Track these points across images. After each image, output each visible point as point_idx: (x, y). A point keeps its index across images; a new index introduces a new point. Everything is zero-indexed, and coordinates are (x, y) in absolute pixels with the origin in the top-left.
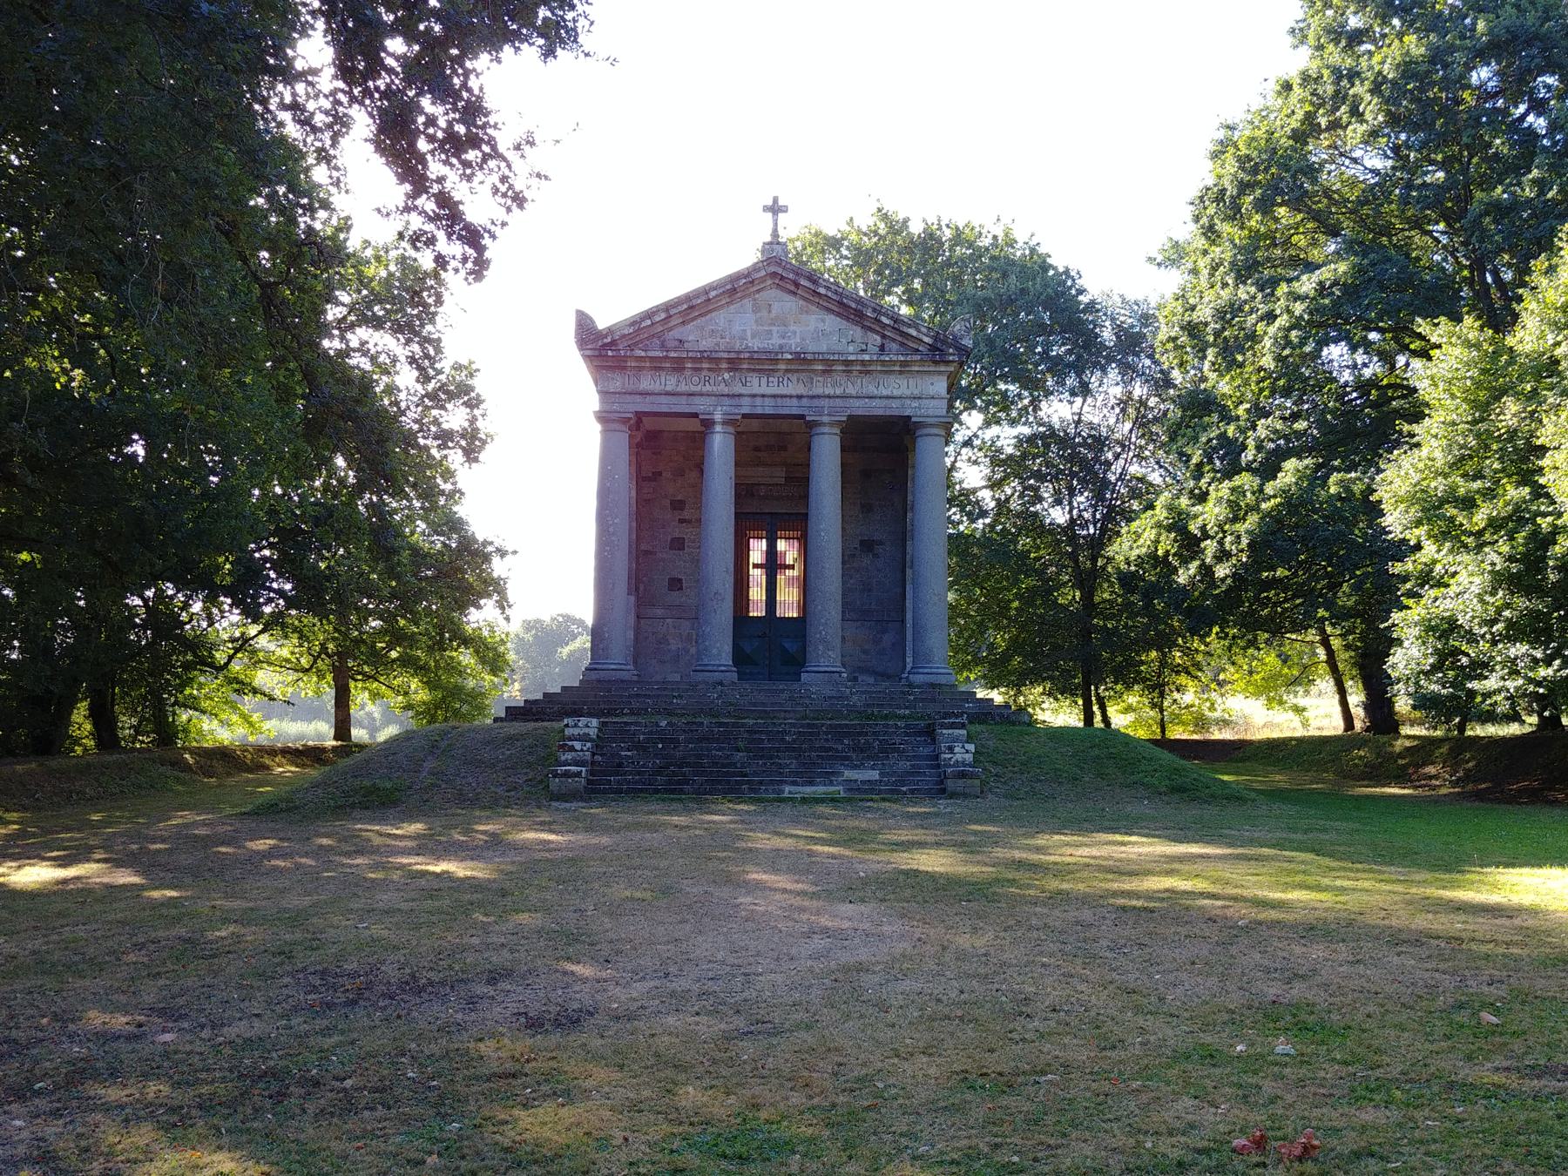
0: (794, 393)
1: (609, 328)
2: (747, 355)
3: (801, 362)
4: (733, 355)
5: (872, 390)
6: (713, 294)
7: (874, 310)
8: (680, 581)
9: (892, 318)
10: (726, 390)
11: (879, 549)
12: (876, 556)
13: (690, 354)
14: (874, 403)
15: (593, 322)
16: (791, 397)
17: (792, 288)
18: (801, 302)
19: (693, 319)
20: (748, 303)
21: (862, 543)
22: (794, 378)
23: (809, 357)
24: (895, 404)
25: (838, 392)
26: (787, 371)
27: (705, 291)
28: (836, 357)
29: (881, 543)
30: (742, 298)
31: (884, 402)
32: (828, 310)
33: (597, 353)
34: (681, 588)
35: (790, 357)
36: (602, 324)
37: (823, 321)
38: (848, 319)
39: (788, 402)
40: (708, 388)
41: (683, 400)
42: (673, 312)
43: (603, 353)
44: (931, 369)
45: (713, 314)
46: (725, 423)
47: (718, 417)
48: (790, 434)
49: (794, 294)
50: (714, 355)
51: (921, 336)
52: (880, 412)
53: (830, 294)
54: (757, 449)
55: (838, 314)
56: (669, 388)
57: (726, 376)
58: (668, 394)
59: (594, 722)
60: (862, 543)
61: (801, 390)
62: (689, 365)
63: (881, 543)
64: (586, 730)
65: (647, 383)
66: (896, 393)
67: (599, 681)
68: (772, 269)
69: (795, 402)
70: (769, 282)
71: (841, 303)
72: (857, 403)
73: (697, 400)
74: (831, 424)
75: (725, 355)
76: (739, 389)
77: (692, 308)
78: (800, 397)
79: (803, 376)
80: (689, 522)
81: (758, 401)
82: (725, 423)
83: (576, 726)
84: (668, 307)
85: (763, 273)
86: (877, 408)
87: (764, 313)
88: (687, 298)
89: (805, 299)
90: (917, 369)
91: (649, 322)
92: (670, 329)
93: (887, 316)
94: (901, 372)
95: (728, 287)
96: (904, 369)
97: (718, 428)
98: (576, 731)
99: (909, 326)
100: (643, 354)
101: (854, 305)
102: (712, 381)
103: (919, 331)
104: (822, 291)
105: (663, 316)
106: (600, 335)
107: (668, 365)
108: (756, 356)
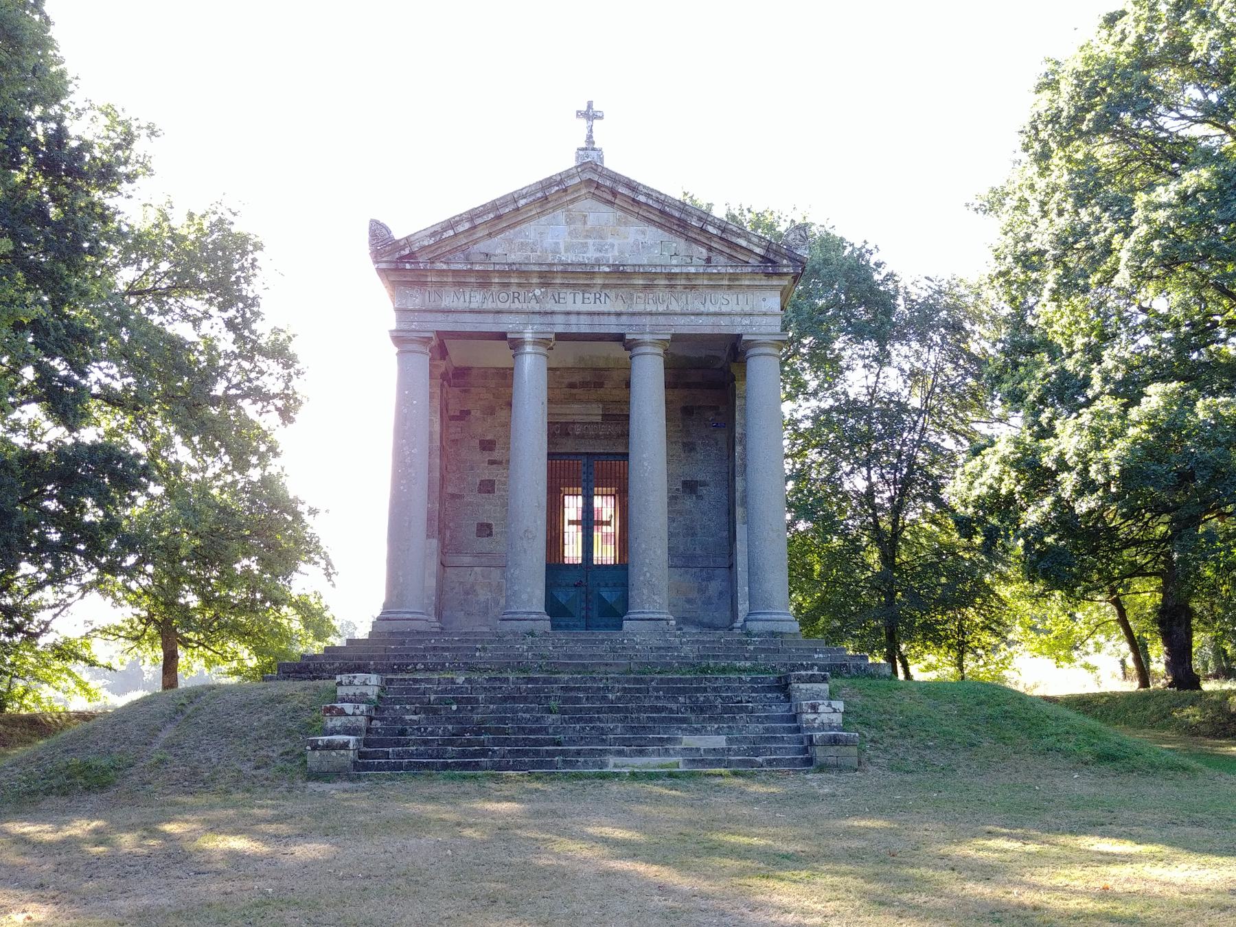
0: (613, 310)
1: (407, 239)
2: (560, 268)
3: (620, 276)
4: (545, 268)
6: (522, 202)
7: (700, 219)
8: (489, 526)
9: (719, 227)
10: (537, 308)
11: (703, 491)
12: (700, 497)
13: (497, 267)
15: (389, 232)
16: (609, 314)
17: (610, 198)
18: (619, 213)
19: (503, 230)
20: (560, 215)
21: (685, 483)
22: (612, 294)
23: (629, 269)
24: (724, 321)
25: (661, 309)
26: (604, 286)
27: (513, 198)
28: (659, 270)
29: (704, 484)
30: (554, 209)
31: (712, 320)
32: (650, 221)
33: (393, 266)
34: (490, 534)
35: (607, 269)
36: (399, 233)
37: (644, 233)
38: (670, 230)
39: (605, 319)
40: (517, 305)
42: (478, 221)
43: (401, 266)
44: (764, 283)
45: (523, 226)
46: (536, 343)
47: (528, 336)
48: (608, 369)
49: (611, 203)
50: (524, 268)
51: (752, 247)
52: (708, 331)
53: (650, 202)
54: (572, 386)
55: (661, 226)
56: (474, 306)
57: (538, 292)
58: (472, 311)
59: (374, 679)
60: (685, 483)
61: (620, 307)
62: (497, 280)
63: (704, 484)
64: (364, 689)
65: (449, 300)
66: (724, 309)
67: (392, 633)
68: (587, 176)
69: (613, 319)
70: (584, 191)
71: (662, 212)
72: (682, 320)
74: (653, 344)
75: (536, 268)
76: (550, 306)
78: (619, 314)
79: (620, 292)
80: (501, 463)
81: (573, 319)
82: (536, 343)
83: (351, 684)
84: (472, 215)
85: (577, 180)
86: (705, 326)
87: (579, 225)
88: (494, 206)
89: (623, 209)
90: (747, 283)
91: (451, 233)
92: (476, 242)
93: (714, 225)
94: (730, 287)
95: (539, 195)
96: (732, 283)
97: (528, 348)
98: (350, 691)
99: (739, 236)
100: (445, 267)
101: (677, 214)
102: (521, 298)
103: (749, 241)
104: (642, 199)
105: (467, 226)
106: (396, 245)
107: (473, 280)
108: (570, 269)
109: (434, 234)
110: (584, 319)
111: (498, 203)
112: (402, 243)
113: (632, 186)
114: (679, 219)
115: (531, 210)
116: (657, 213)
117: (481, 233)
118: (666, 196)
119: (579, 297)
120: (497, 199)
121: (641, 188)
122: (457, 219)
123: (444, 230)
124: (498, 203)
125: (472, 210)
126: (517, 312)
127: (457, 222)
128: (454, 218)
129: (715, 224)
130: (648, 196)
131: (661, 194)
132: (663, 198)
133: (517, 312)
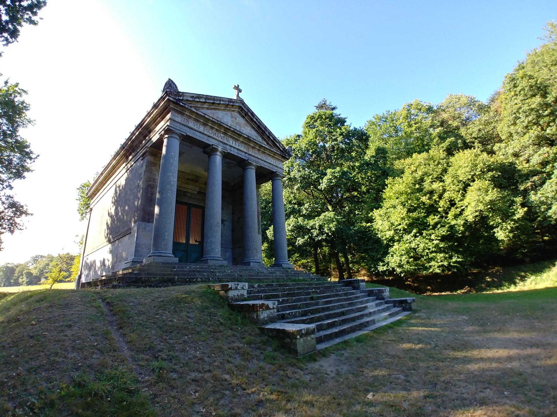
0: (244, 151)
2: (233, 130)
4: (228, 127)
5: (264, 159)
10: (221, 140)
13: (213, 120)
14: (266, 164)
16: (243, 152)
22: (243, 145)
24: (271, 166)
25: (256, 156)
26: (242, 142)
31: (268, 165)
39: (241, 153)
40: (214, 137)
41: (206, 137)
42: (208, 101)
46: (221, 152)
47: (220, 149)
50: (221, 124)
58: (200, 132)
61: (245, 150)
65: (191, 124)
73: (211, 139)
75: (226, 126)
76: (226, 142)
77: (213, 103)
78: (245, 153)
81: (232, 149)
88: (214, 98)
91: (198, 100)
92: (203, 108)
94: (273, 157)
97: (218, 153)
102: (216, 135)
105: (204, 101)
107: (202, 121)
108: (236, 131)
109: (192, 97)
110: (235, 150)
117: (206, 106)
119: (234, 142)
125: (208, 96)
126: (216, 139)
127: (201, 97)
133: (216, 139)
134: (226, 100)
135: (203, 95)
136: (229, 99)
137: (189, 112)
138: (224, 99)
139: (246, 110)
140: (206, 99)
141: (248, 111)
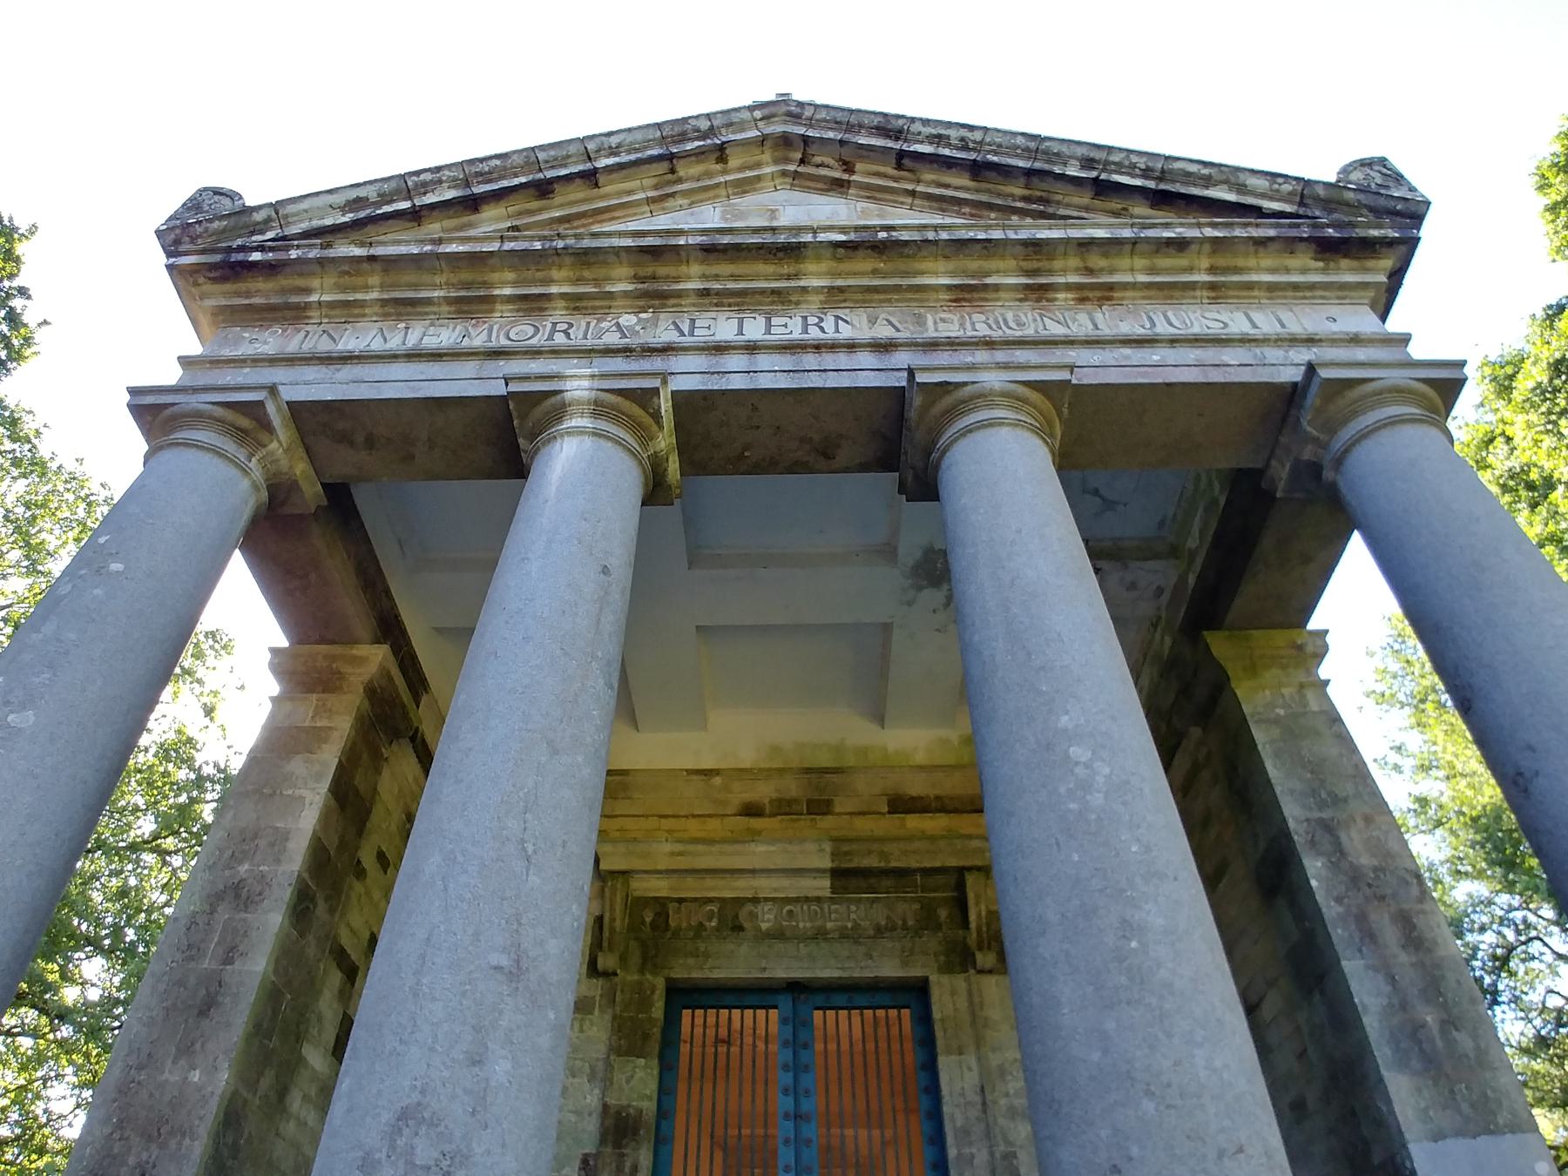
1: (276, 206)
71: (978, 169)
91: (405, 205)
93: (1131, 169)
111: (542, 156)
112: (258, 217)
113: (889, 126)
114: (1029, 173)
115: (630, 192)
116: (965, 181)
118: (986, 129)
120: (542, 148)
121: (917, 127)
122: (427, 177)
123: (386, 198)
124: (542, 156)
125: (472, 162)
127: (424, 184)
128: (418, 173)
129: (1133, 166)
130: (938, 139)
131: (971, 128)
132: (978, 136)
134: (639, 136)
135: (438, 169)
136: (659, 126)
137: (330, 280)
138: (614, 141)
139: (831, 135)
140: (467, 184)
141: (849, 128)
